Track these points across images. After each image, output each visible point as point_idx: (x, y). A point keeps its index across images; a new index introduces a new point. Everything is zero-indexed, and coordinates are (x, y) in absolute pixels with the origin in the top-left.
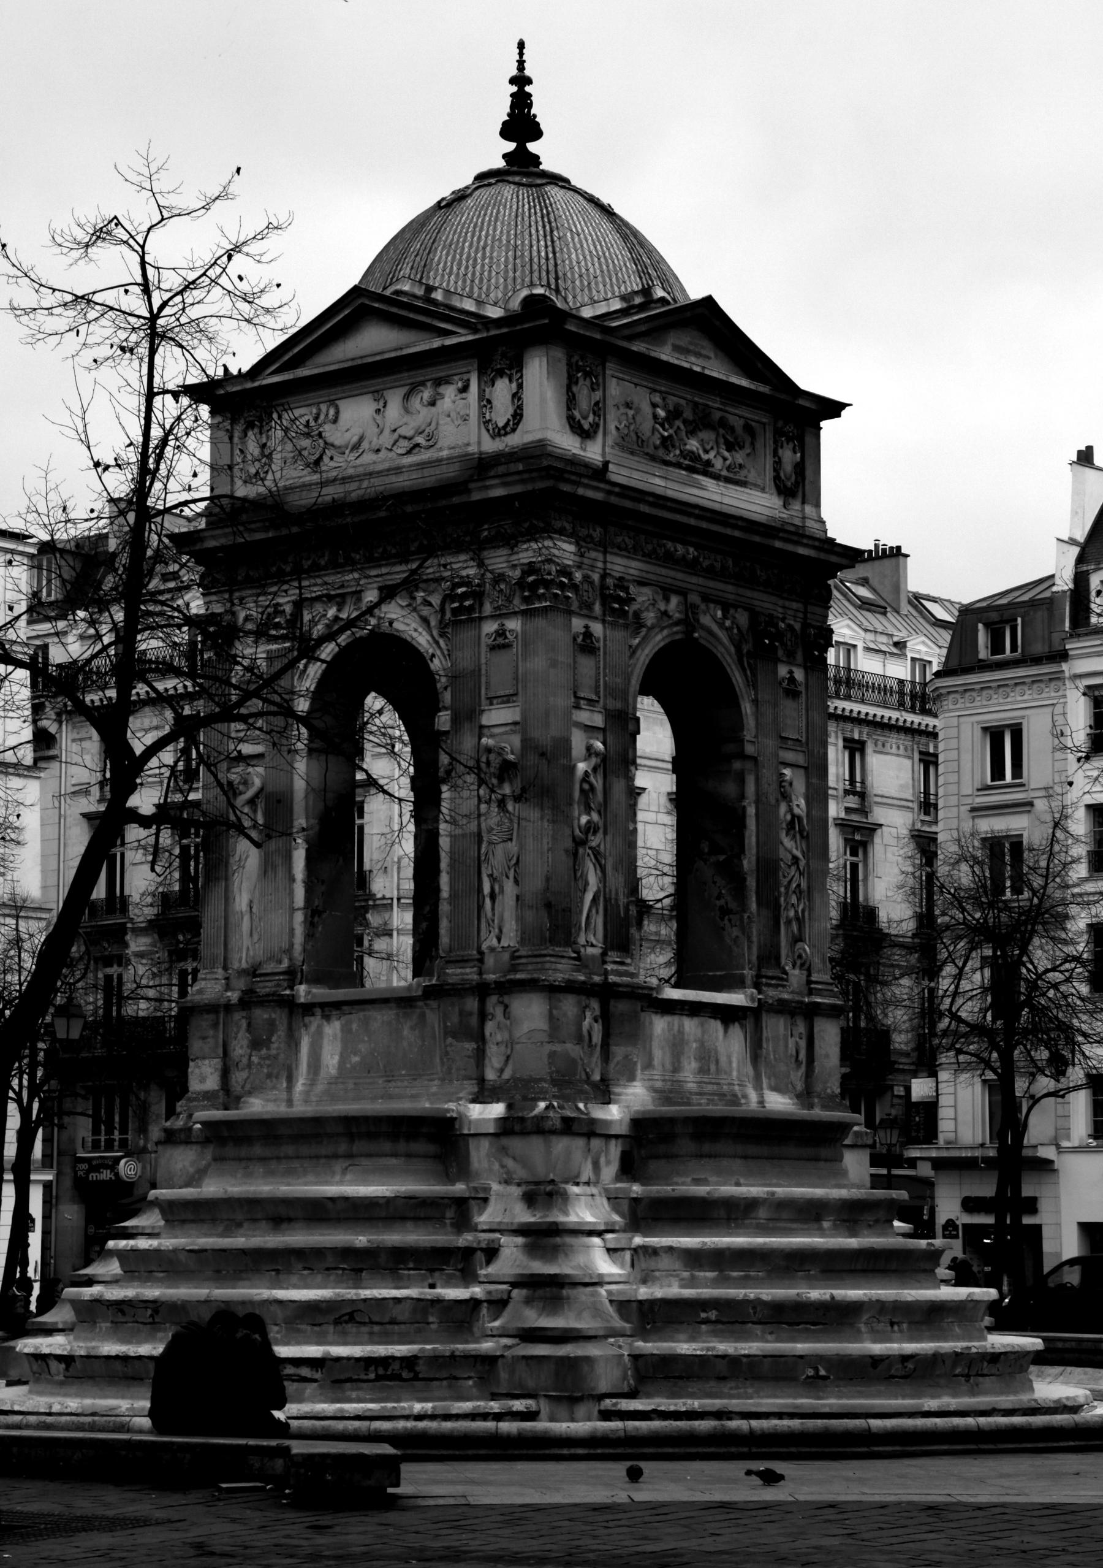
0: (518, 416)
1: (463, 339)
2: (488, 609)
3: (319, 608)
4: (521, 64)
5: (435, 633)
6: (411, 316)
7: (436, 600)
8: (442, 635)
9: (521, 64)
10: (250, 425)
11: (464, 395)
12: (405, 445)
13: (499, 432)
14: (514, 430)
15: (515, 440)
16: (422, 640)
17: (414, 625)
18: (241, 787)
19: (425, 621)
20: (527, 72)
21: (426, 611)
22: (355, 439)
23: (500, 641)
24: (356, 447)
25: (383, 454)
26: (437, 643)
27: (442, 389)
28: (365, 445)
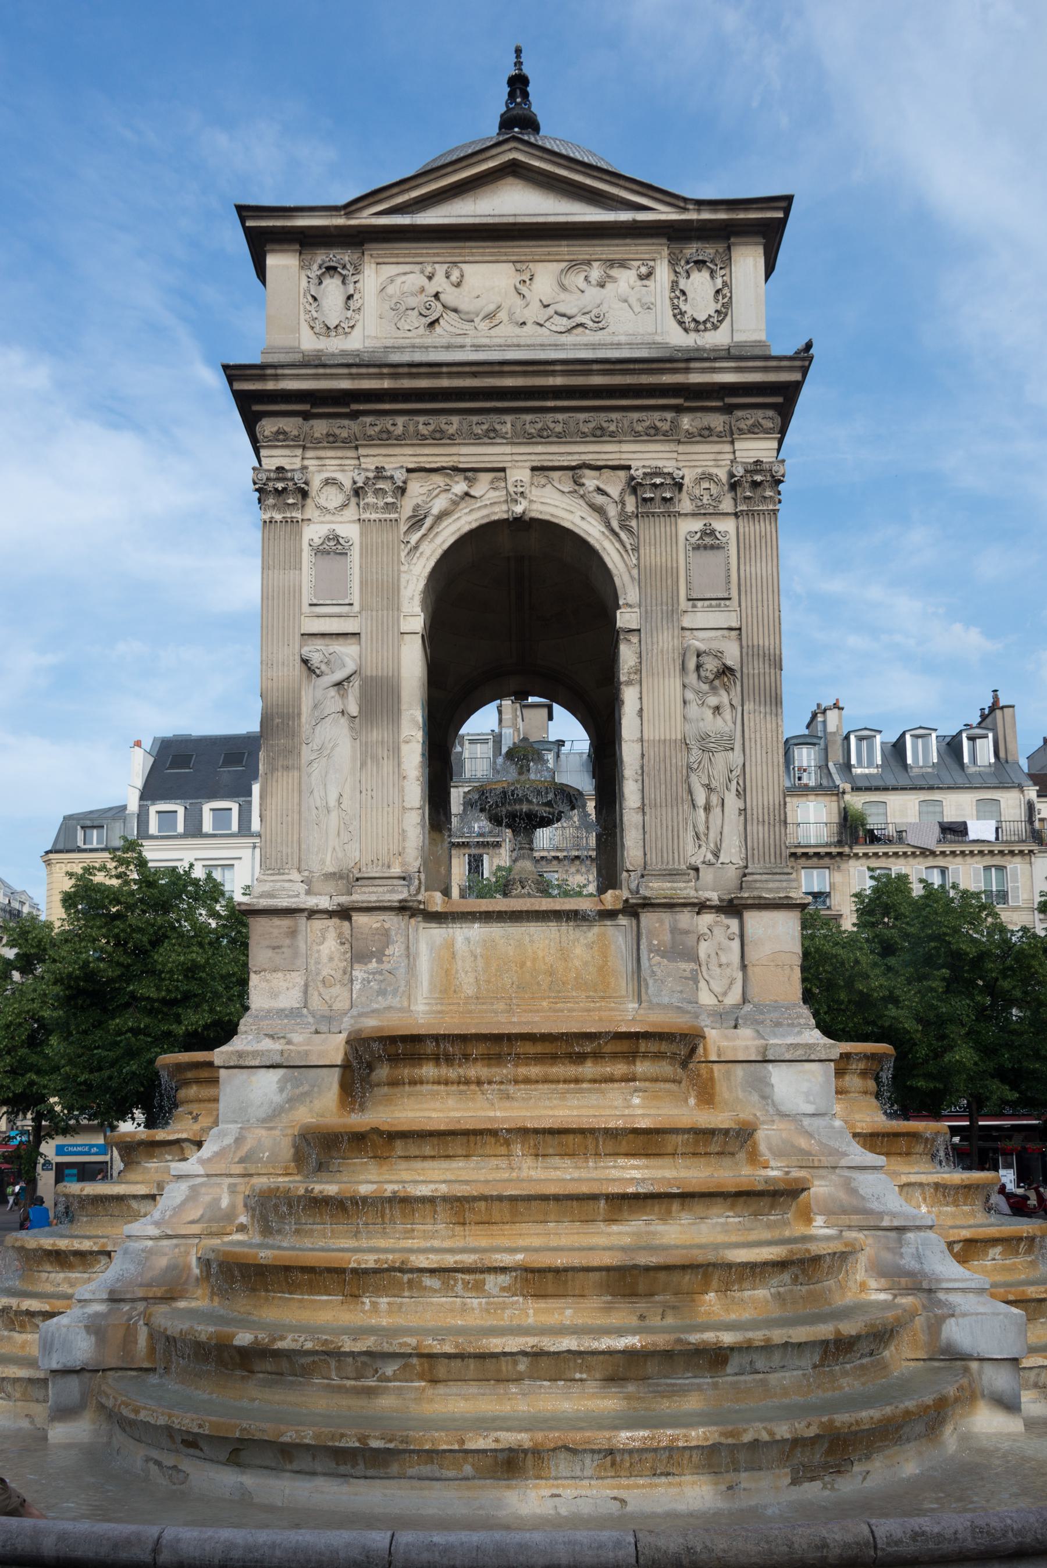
0: (722, 314)
1: (663, 217)
2: (686, 505)
3: (438, 480)
4: (518, 64)
5: (615, 524)
6: (589, 182)
7: (614, 491)
8: (623, 527)
9: (518, 64)
10: (331, 270)
11: (645, 282)
12: (564, 323)
13: (699, 326)
14: (715, 328)
15: (718, 338)
16: (591, 530)
17: (580, 513)
18: (323, 667)
19: (599, 510)
20: (526, 70)
21: (600, 499)
22: (492, 307)
23: (708, 540)
24: (490, 316)
25: (529, 328)
26: (616, 534)
27: (615, 272)
28: (502, 315)
